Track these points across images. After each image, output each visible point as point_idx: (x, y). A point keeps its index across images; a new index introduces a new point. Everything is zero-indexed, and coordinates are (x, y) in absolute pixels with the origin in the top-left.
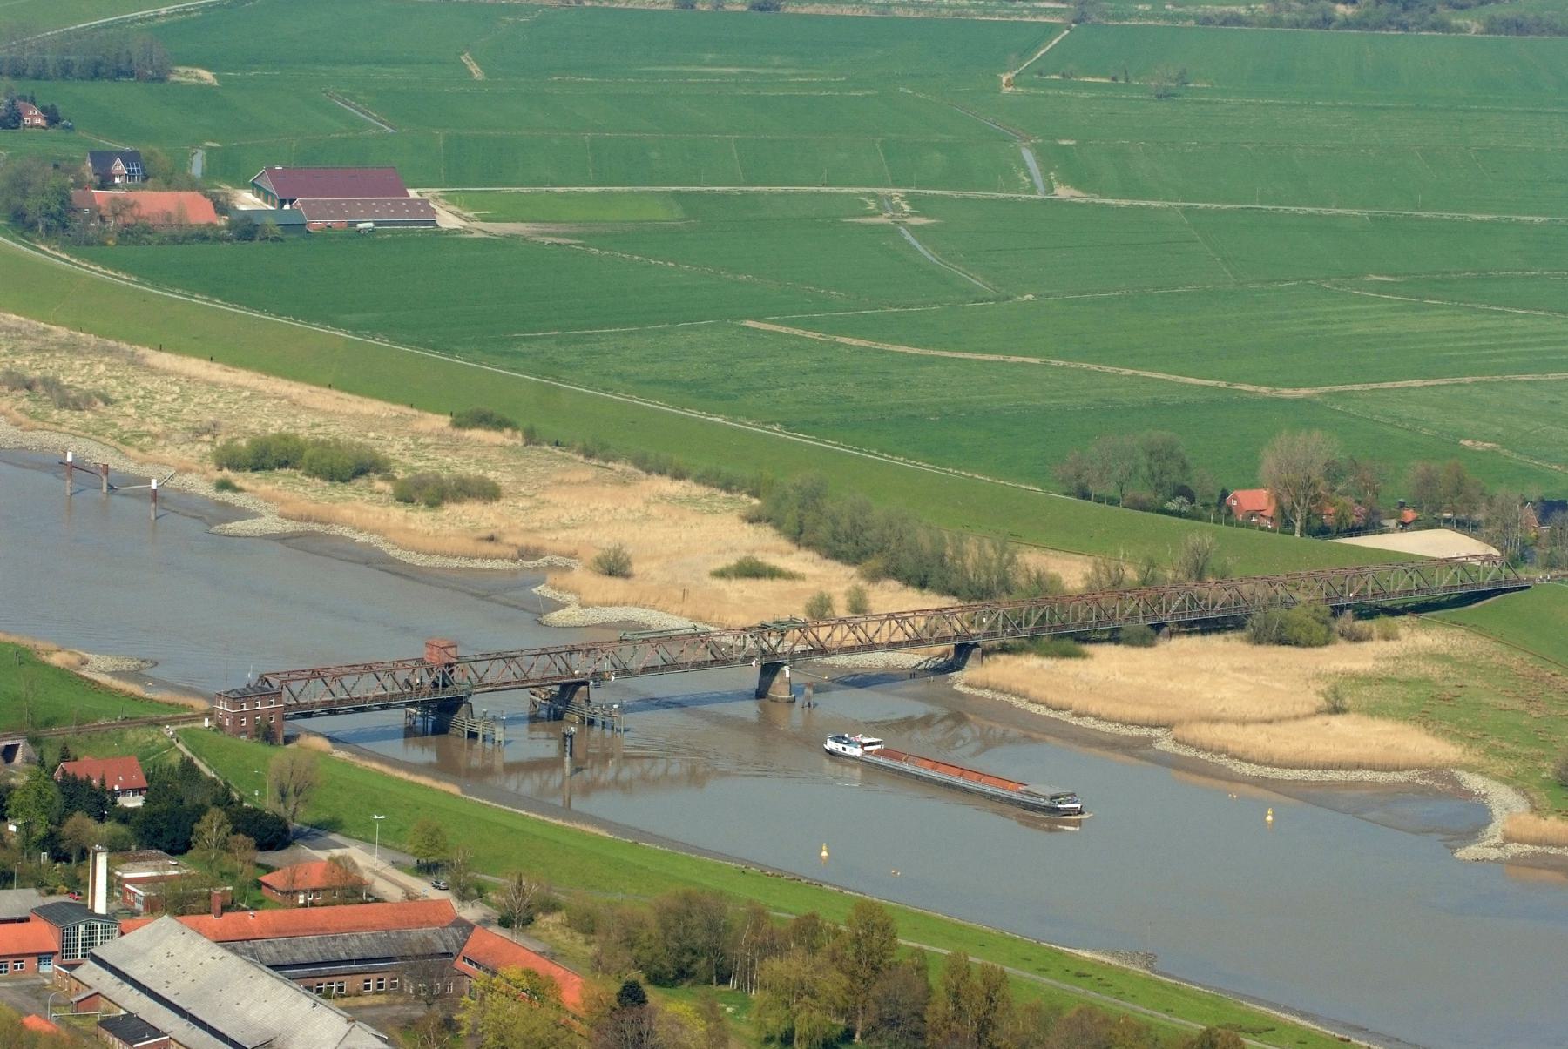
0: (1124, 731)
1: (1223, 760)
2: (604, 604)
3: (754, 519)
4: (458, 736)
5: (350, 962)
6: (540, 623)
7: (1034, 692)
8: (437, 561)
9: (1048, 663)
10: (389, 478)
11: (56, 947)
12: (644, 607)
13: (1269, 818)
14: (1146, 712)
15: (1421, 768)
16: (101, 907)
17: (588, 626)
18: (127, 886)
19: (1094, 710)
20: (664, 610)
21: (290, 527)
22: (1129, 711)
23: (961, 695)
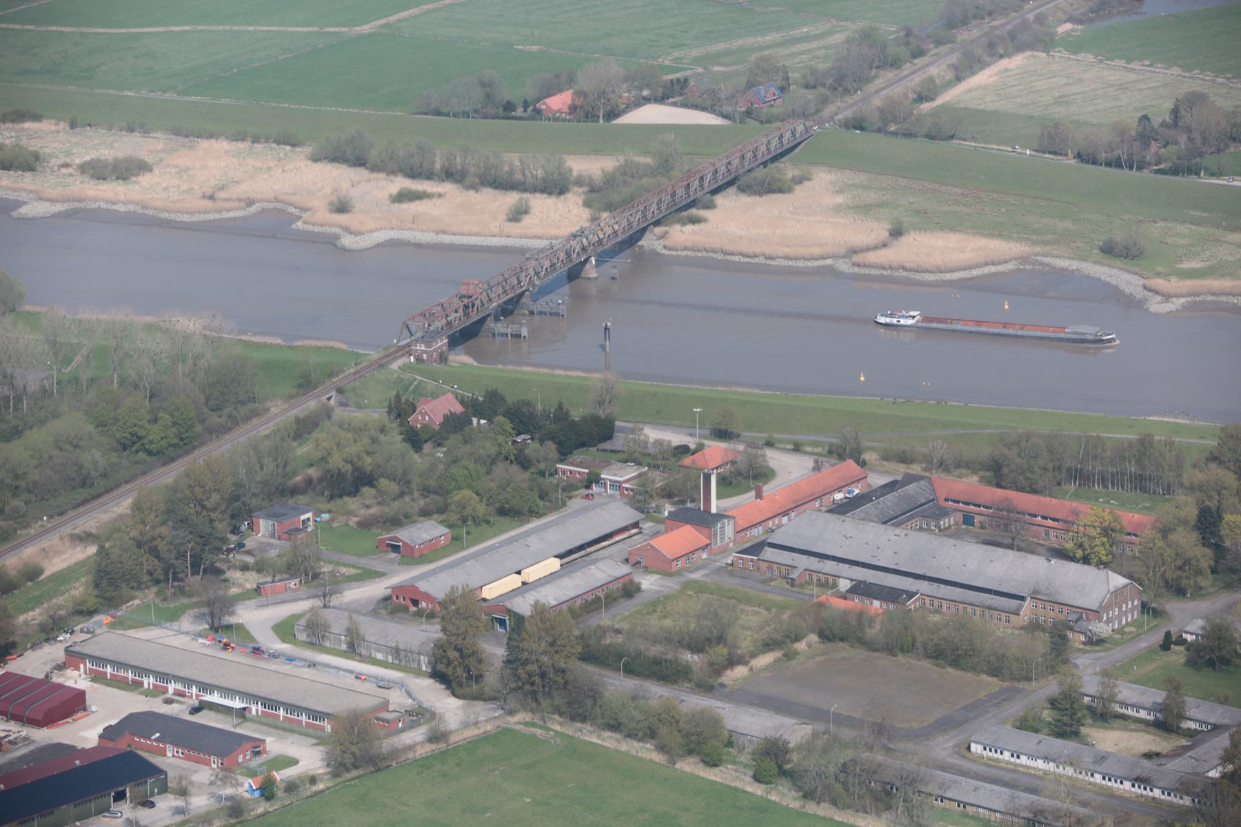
0: (810, 264)
1: (904, 274)
2: (372, 231)
3: (315, 159)
4: (488, 336)
5: (898, 517)
6: (344, 249)
7: (730, 248)
8: (196, 218)
9: (689, 228)
10: (66, 165)
11: (708, 542)
12: (392, 229)
13: (1006, 307)
14: (816, 251)
15: (1016, 259)
16: (714, 510)
17: (375, 246)
18: (624, 485)
19: (780, 254)
20: (411, 229)
21: (58, 208)
22: (803, 251)
23: (663, 255)
